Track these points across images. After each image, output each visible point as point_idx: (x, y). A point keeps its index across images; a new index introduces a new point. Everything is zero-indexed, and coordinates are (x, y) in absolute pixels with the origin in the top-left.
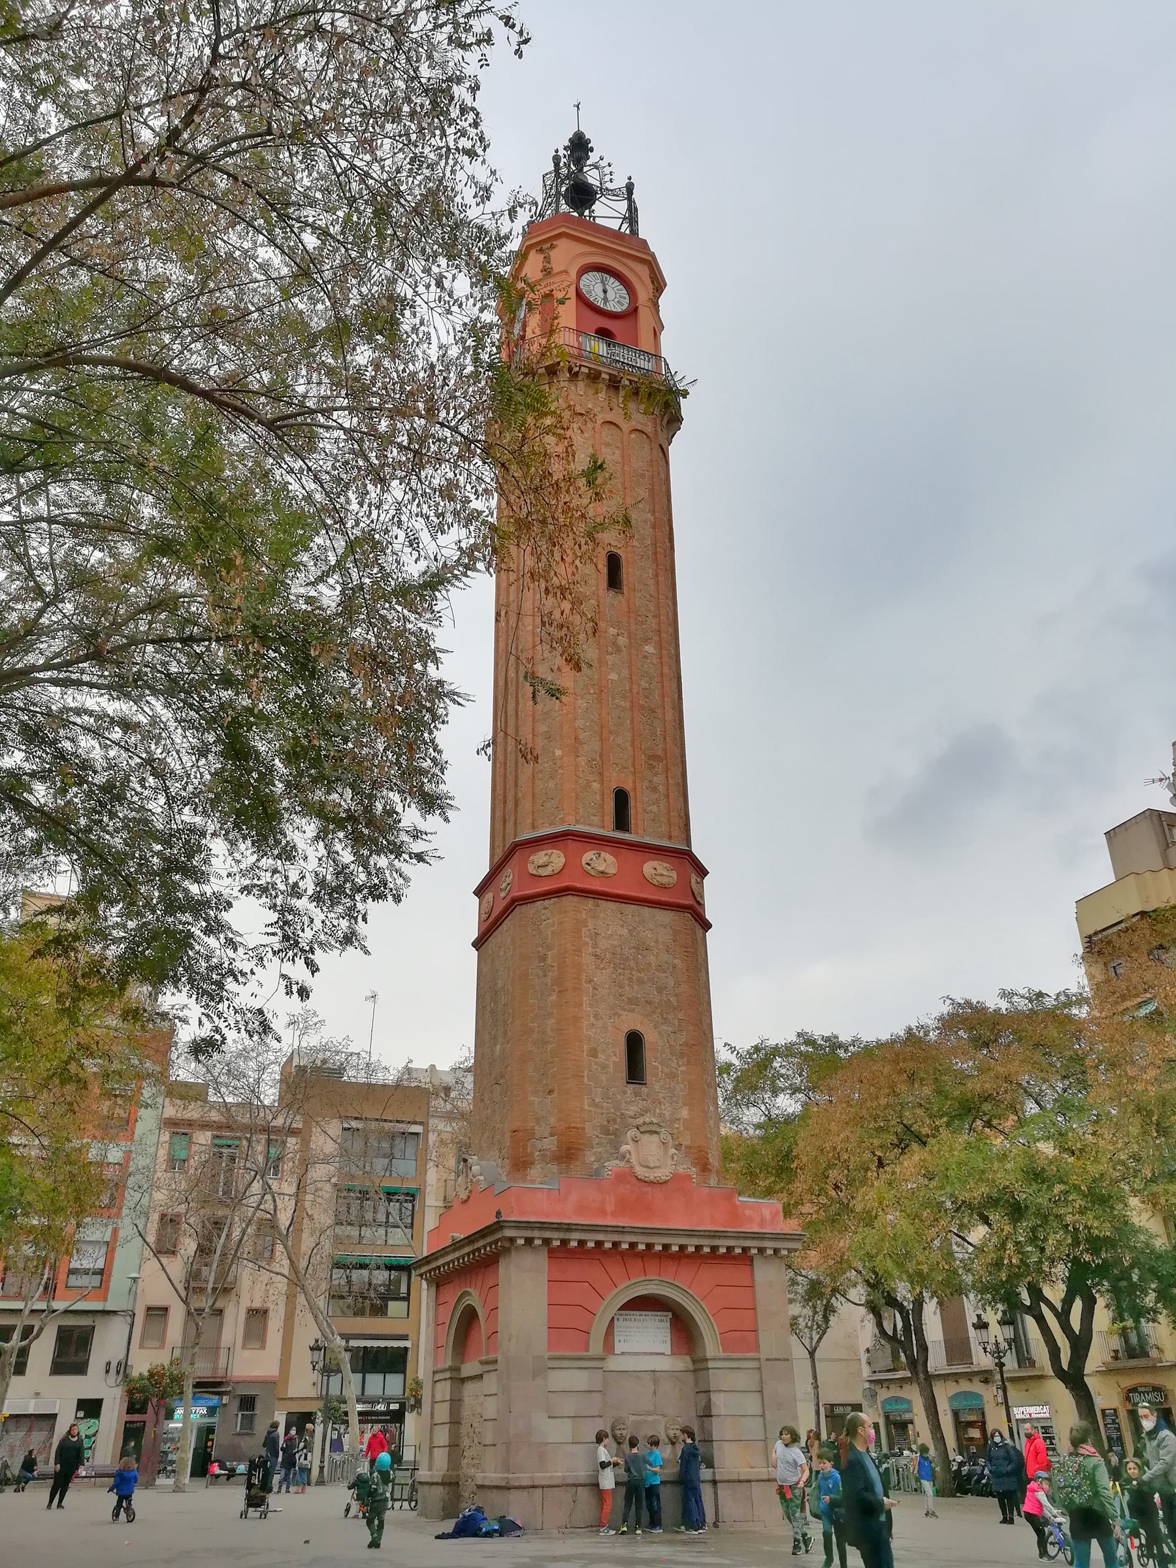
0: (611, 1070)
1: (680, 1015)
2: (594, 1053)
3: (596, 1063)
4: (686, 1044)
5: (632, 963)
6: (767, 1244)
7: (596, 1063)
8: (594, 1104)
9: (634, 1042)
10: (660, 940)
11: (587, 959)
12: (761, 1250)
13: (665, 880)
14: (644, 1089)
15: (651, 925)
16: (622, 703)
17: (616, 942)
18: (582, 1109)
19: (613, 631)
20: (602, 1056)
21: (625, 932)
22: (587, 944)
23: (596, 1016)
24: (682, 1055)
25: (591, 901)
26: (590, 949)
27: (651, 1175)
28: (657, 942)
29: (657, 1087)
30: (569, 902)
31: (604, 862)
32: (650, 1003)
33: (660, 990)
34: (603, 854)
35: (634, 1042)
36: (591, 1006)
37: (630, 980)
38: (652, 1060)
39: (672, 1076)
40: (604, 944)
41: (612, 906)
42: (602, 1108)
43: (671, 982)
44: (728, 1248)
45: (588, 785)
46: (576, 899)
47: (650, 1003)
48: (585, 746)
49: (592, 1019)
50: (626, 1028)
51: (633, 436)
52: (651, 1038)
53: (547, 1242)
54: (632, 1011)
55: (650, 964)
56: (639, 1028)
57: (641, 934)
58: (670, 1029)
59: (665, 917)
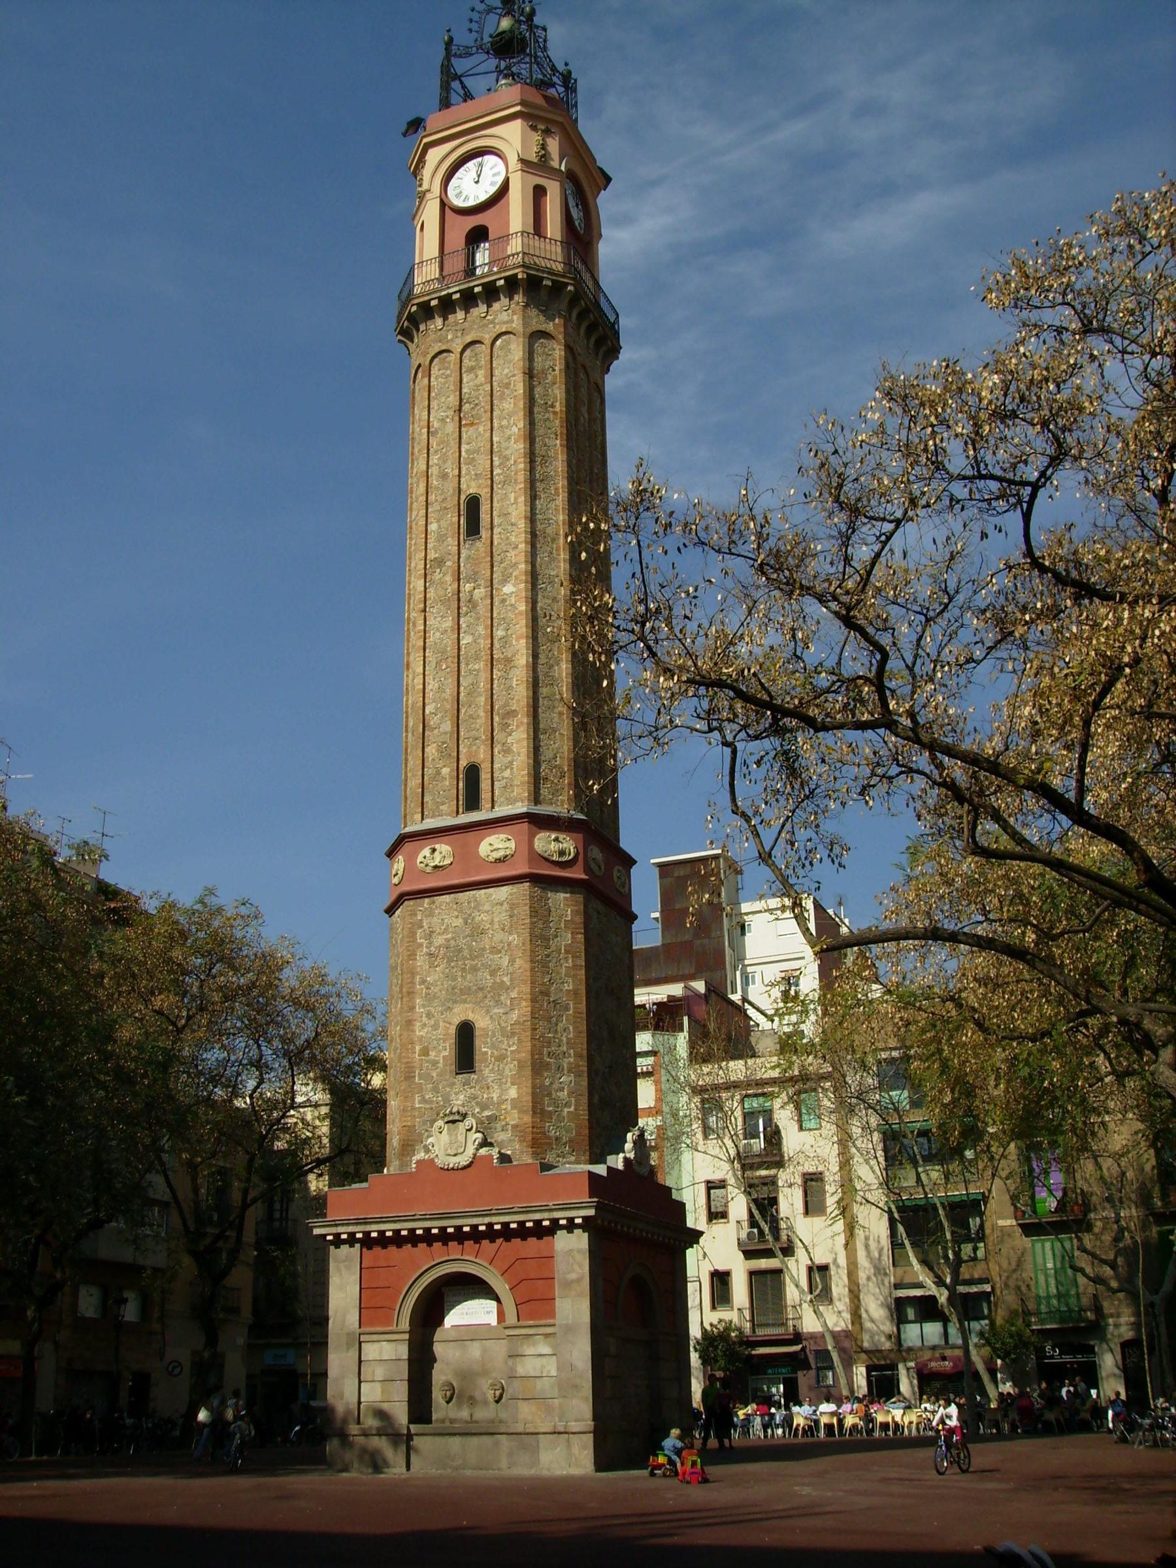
0: (440, 1065)
1: (514, 994)
2: (425, 1052)
3: (427, 1061)
4: (517, 1023)
5: (466, 953)
6: (556, 1215)
7: (427, 1061)
8: (423, 1100)
9: (466, 1034)
10: (496, 920)
11: (421, 961)
12: (555, 1221)
13: (500, 854)
14: (473, 1076)
15: (486, 907)
16: (476, 667)
17: (450, 936)
18: (413, 1108)
19: (468, 587)
20: (432, 1054)
21: (459, 922)
22: (421, 945)
23: (429, 1015)
24: (513, 1034)
25: (427, 900)
26: (425, 950)
27: (453, 1162)
28: (492, 923)
29: (486, 1072)
30: (408, 904)
31: (442, 852)
32: (481, 989)
33: (493, 973)
34: (437, 846)
35: (466, 1034)
36: (424, 1006)
37: (463, 970)
38: (482, 1047)
39: (501, 1058)
40: (439, 940)
41: (446, 898)
42: (432, 1102)
43: (505, 961)
44: (519, 1223)
45: (438, 773)
46: (412, 903)
47: (481, 989)
48: (436, 731)
49: (424, 1019)
50: (456, 1021)
51: (498, 343)
52: (481, 1022)
53: (352, 1235)
54: (465, 1001)
55: (484, 949)
56: (471, 1017)
57: (478, 919)
58: (501, 1011)
59: (503, 892)
